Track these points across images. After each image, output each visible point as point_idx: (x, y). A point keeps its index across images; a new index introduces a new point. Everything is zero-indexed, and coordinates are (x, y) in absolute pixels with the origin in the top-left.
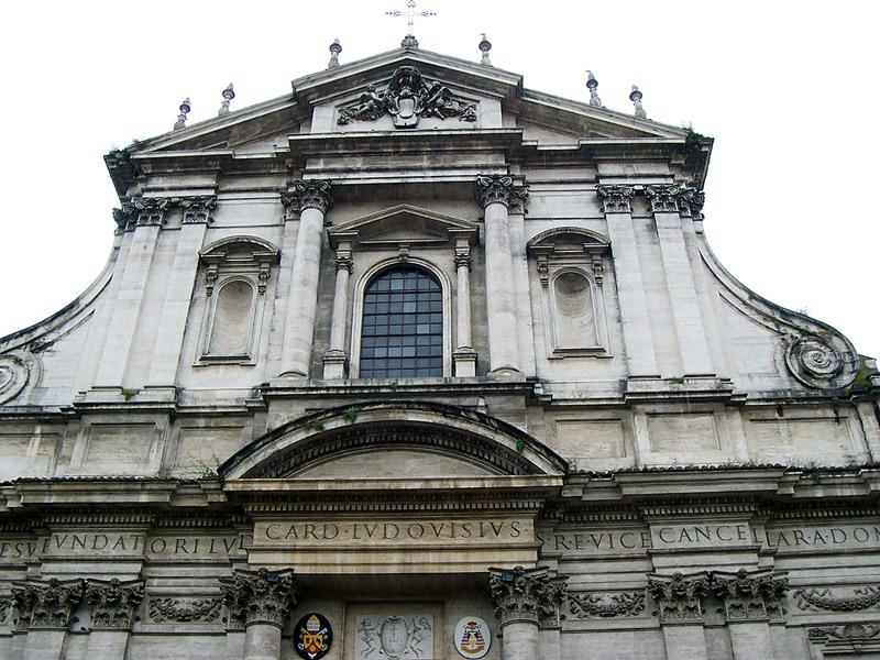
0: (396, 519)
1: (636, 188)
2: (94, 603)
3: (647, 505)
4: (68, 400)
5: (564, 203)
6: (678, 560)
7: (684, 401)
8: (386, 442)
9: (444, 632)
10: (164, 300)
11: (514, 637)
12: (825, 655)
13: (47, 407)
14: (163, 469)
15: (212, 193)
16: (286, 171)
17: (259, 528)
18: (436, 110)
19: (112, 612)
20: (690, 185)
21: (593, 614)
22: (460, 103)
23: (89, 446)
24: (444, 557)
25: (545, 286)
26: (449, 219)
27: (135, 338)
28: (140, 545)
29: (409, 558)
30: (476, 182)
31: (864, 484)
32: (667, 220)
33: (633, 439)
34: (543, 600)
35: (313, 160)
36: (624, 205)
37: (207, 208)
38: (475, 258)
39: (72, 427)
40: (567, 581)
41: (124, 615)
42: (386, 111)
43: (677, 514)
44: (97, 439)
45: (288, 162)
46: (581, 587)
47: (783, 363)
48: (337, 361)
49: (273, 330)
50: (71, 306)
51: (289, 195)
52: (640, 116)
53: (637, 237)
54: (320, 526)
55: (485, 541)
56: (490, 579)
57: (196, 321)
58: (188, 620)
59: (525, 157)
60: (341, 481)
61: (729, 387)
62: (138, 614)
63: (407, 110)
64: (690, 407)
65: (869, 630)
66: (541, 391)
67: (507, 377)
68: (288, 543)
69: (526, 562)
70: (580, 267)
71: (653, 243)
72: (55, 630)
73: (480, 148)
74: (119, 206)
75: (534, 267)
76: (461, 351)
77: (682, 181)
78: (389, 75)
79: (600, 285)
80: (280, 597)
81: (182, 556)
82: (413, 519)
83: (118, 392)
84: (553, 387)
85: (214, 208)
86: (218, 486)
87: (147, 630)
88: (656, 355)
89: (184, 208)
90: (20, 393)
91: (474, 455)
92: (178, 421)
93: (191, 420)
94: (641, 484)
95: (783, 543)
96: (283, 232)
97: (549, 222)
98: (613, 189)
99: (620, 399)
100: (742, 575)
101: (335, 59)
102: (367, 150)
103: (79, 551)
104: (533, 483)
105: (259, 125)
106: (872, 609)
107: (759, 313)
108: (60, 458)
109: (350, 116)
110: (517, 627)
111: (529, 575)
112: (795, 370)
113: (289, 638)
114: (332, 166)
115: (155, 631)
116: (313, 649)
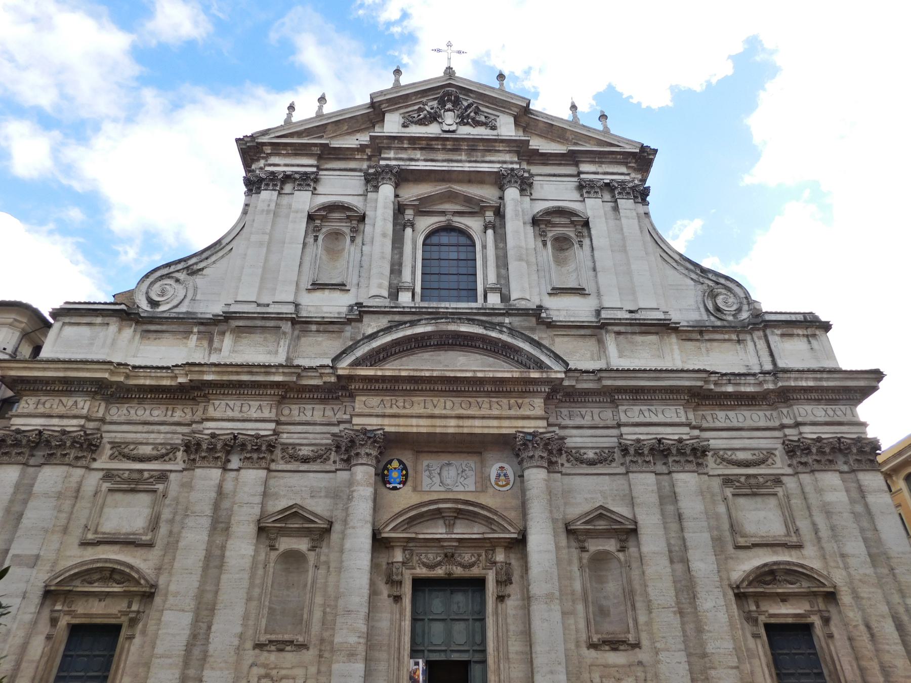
2: (242, 450)
4: (216, 309)
8: (445, 344)
9: (482, 473)
10: (284, 243)
12: (734, 495)
13: (201, 313)
14: (288, 359)
15: (314, 169)
19: (255, 456)
20: (641, 181)
22: (486, 117)
25: (545, 244)
27: (264, 268)
28: (274, 411)
29: (461, 422)
31: (760, 384)
32: (626, 204)
34: (550, 452)
36: (597, 192)
37: (312, 180)
39: (222, 327)
40: (566, 441)
42: (435, 119)
43: (637, 399)
45: (368, 151)
46: (573, 445)
48: (407, 289)
52: (606, 131)
53: (605, 214)
54: (401, 399)
55: (512, 413)
56: (516, 438)
58: (308, 462)
59: (530, 157)
61: (668, 317)
63: (449, 119)
64: (644, 328)
65: (761, 480)
67: (523, 304)
68: (379, 411)
69: (540, 428)
70: (568, 233)
75: (537, 232)
78: (437, 94)
79: (581, 246)
81: (303, 418)
83: (255, 305)
84: (551, 313)
85: (316, 180)
86: (331, 371)
87: (280, 469)
89: (296, 179)
90: (181, 302)
92: (298, 326)
94: (615, 378)
96: (366, 200)
97: (546, 202)
98: (590, 181)
99: (597, 322)
100: (680, 441)
101: (397, 81)
102: (424, 146)
103: (230, 414)
104: (545, 375)
106: (763, 466)
110: (534, 471)
112: (710, 307)
115: (285, 469)
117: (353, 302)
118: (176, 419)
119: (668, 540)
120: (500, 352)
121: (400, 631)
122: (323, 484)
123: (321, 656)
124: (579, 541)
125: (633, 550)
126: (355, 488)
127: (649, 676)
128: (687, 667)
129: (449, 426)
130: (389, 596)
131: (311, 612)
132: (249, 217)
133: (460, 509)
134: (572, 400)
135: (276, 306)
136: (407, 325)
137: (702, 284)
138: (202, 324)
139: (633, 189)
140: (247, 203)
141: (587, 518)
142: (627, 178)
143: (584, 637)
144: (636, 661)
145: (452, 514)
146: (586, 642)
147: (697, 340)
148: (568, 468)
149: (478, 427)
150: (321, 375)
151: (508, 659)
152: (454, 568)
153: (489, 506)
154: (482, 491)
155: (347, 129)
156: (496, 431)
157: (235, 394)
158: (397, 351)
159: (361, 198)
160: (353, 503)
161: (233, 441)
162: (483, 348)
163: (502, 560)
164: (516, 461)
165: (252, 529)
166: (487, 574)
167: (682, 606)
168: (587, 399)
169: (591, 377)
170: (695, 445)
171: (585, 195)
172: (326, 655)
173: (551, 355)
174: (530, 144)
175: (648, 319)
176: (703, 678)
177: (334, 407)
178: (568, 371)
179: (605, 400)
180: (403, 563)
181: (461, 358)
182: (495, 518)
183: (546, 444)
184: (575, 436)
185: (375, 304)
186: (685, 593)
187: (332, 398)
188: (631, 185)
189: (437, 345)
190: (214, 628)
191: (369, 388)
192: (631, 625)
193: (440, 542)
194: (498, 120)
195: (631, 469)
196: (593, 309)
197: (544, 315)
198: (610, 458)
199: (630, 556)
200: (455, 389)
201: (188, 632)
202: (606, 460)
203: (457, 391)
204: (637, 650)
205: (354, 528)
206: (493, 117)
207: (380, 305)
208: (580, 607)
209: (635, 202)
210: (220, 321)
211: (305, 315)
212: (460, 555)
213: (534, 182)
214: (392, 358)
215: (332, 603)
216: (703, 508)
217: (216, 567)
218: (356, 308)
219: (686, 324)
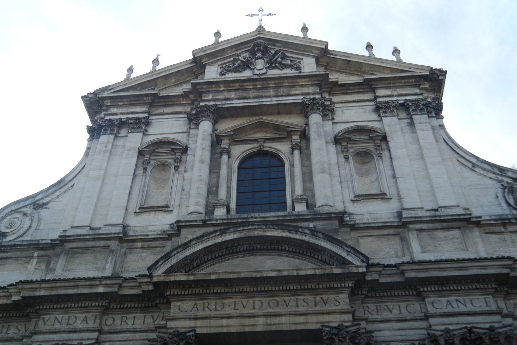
0: (261, 297)
1: (400, 102)
4: (55, 236)
5: (355, 113)
6: (446, 320)
8: (253, 250)
14: (113, 273)
15: (146, 115)
16: (190, 102)
17: (173, 306)
20: (433, 99)
22: (291, 61)
24: (293, 319)
25: (347, 158)
26: (288, 123)
27: (98, 198)
28: (98, 321)
29: (269, 320)
32: (419, 119)
33: (409, 246)
35: (205, 95)
36: (391, 111)
37: (144, 123)
39: (58, 250)
40: (374, 334)
43: (443, 290)
44: (73, 257)
46: (382, 339)
48: (222, 206)
49: (183, 190)
50: (60, 182)
52: (399, 61)
53: (402, 129)
54: (213, 302)
55: (318, 308)
56: (322, 333)
57: (137, 187)
60: (225, 273)
61: (469, 212)
63: (260, 65)
64: (445, 224)
66: (348, 219)
67: (327, 209)
68: (192, 314)
69: (346, 322)
71: (412, 133)
73: (304, 83)
74: (91, 125)
76: (297, 197)
77: (428, 97)
79: (381, 157)
81: (125, 327)
82: (272, 297)
83: (89, 228)
84: (355, 217)
85: (148, 123)
86: (148, 280)
88: (420, 196)
89: (130, 124)
90: (25, 232)
91: (309, 256)
92: (125, 245)
93: (131, 244)
96: (189, 136)
98: (386, 102)
99: (398, 222)
100: (492, 329)
102: (237, 88)
103: (57, 326)
104: (346, 271)
109: (227, 70)
111: (348, 329)
114: (217, 97)
117: (173, 221)
118: (10, 335)
120: (305, 253)
134: (378, 295)
135: (107, 228)
136: (217, 234)
137: (502, 181)
138: (42, 249)
139: (427, 105)
140: (89, 146)
142: (421, 97)
147: (502, 232)
155: (175, 82)
157: (63, 308)
158: (210, 258)
159: (185, 135)
162: (288, 251)
169: (394, 271)
170: (508, 333)
173: (352, 251)
174: (330, 77)
175: (447, 216)
178: (369, 266)
181: (268, 262)
184: (384, 330)
185: (192, 219)
187: (152, 306)
188: (424, 102)
189: (247, 250)
191: (183, 293)
194: (302, 62)
196: (395, 211)
206: (297, 60)
209: (429, 117)
210: (57, 245)
211: (132, 234)
213: (335, 109)
214: (205, 265)
218: (175, 225)
219: (488, 218)
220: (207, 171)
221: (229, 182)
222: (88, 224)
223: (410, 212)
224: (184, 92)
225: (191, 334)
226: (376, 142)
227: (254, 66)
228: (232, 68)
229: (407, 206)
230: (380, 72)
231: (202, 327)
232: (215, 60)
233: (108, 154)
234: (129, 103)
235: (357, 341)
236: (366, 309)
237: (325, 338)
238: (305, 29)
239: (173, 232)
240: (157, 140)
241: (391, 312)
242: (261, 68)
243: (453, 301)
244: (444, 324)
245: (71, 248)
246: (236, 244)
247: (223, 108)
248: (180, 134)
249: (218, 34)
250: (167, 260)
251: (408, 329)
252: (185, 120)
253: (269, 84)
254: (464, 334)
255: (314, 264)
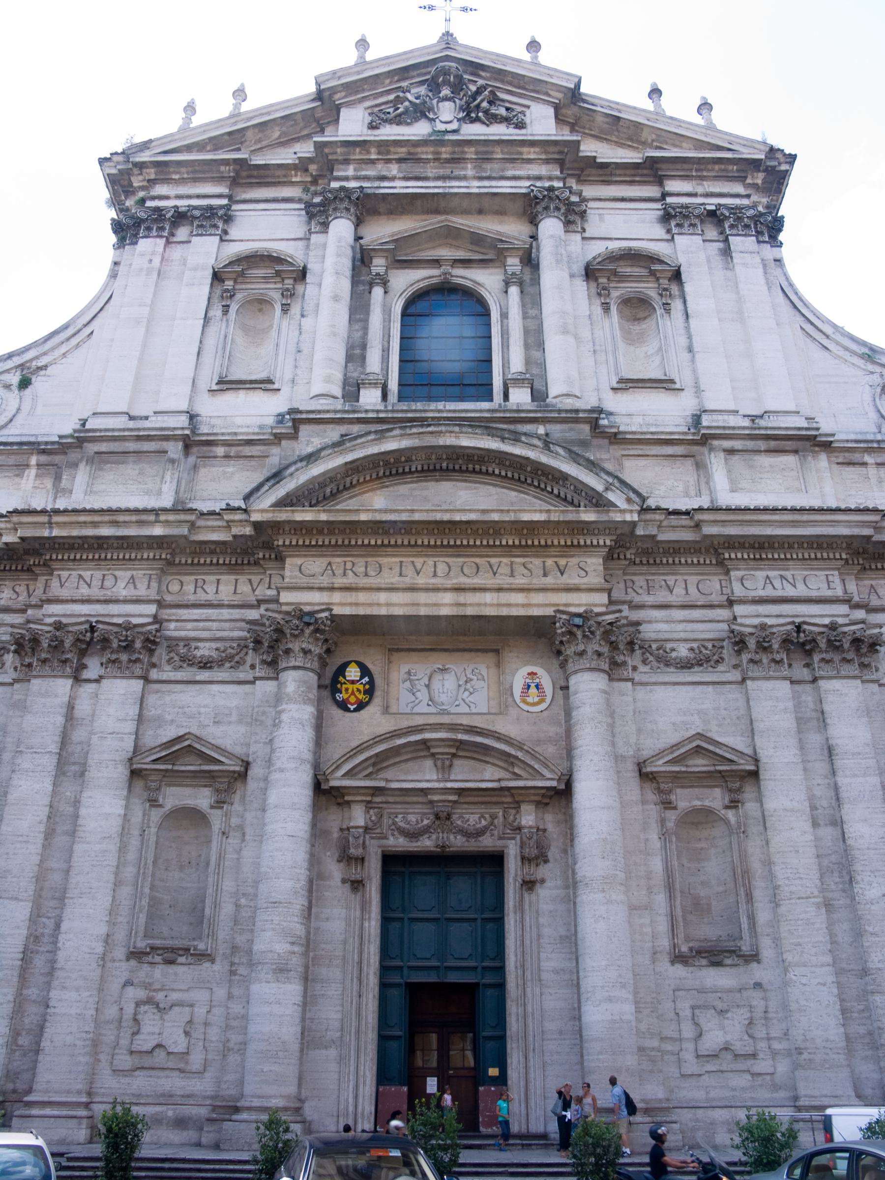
1: (709, 208)
2: (104, 649)
3: (728, 548)
4: (67, 427)
6: (762, 609)
7: (768, 437)
8: (435, 470)
11: (582, 687)
14: (177, 501)
15: (225, 202)
16: (309, 179)
18: (480, 114)
19: (124, 657)
20: (767, 207)
21: (667, 665)
22: (507, 109)
23: (93, 478)
24: (505, 597)
25: (606, 308)
28: (154, 584)
29: (462, 598)
30: (528, 194)
34: (614, 646)
35: (341, 167)
36: (691, 225)
37: (221, 218)
38: (527, 277)
39: (73, 455)
40: (641, 628)
41: (138, 660)
43: (761, 559)
44: (101, 469)
45: (313, 168)
46: (653, 636)
47: (871, 404)
48: (375, 385)
50: (65, 327)
51: (315, 205)
52: (710, 127)
53: (708, 261)
54: (360, 562)
55: (549, 581)
58: (211, 668)
61: (815, 425)
62: (154, 660)
64: (773, 444)
67: (569, 403)
68: (325, 581)
69: (596, 605)
72: (61, 677)
73: (532, 156)
75: (594, 290)
76: (514, 376)
78: (426, 74)
79: (668, 311)
80: (317, 639)
81: (202, 597)
83: (127, 418)
84: (618, 420)
85: (228, 219)
88: (733, 388)
89: (194, 218)
90: (11, 420)
93: (205, 448)
95: (873, 597)
96: (307, 247)
98: (682, 207)
99: (694, 434)
100: (833, 627)
102: (403, 156)
103: (84, 591)
104: (604, 517)
105: (277, 128)
107: (846, 349)
108: (58, 490)
110: (587, 676)
111: (600, 619)
113: (326, 687)
114: (364, 173)
115: (173, 679)
116: (353, 699)
117: (284, 409)
119: (809, 789)
120: (529, 481)
121: (361, 937)
122: (234, 703)
123: (232, 973)
124: (660, 791)
125: (750, 807)
126: (284, 706)
127: (773, 1005)
128: (835, 991)
129: (442, 605)
130: (344, 881)
131: (216, 905)
132: (120, 281)
133: (461, 742)
134: (651, 561)
135: (160, 418)
138: (44, 452)
139: (757, 219)
140: (117, 260)
141: (675, 755)
142: (745, 202)
143: (664, 943)
144: (752, 982)
145: (447, 750)
146: (670, 953)
148: (643, 673)
149: (491, 605)
150: (229, 526)
151: (540, 980)
152: (452, 837)
153: (512, 736)
154: (501, 713)
155: (280, 137)
156: (521, 612)
158: (354, 482)
159: (301, 244)
160: (281, 731)
161: (88, 634)
162: (500, 475)
163: (530, 823)
164: (555, 663)
165: (121, 773)
166: (507, 847)
167: (830, 895)
168: (677, 560)
169: (684, 521)
170: (858, 635)
171: (675, 230)
172: (242, 970)
174: (582, 148)
175: (779, 428)
176: (862, 1007)
177: (253, 578)
179: (708, 562)
180: (366, 829)
181: (462, 493)
182: (520, 754)
183: (606, 634)
184: (657, 622)
185: (319, 408)
186: (836, 874)
187: (249, 563)
188: (751, 212)
189: (423, 471)
190: (64, 926)
192: (745, 926)
193: (426, 795)
194: (528, 112)
195: (750, 674)
196: (689, 413)
197: (604, 422)
198: (715, 657)
199: (746, 816)
200: (452, 543)
201: (25, 932)
202: (708, 660)
203: (455, 546)
204: (754, 965)
205: (282, 770)
206: (519, 109)
207: (326, 408)
208: (660, 899)
209: (759, 242)
210: (70, 446)
211: (206, 431)
212: (461, 817)
213: (588, 211)
214: (346, 494)
215: (251, 891)
216: (869, 736)
217: (66, 833)
218: (288, 417)
220: (347, 317)
221: (386, 339)
222: (125, 410)
223: (715, 417)
224: (299, 158)
225: (323, 615)
226: (661, 281)
227: (435, 114)
228: (392, 115)
229: (710, 406)
230: (675, 146)
231: (342, 604)
232: (359, 96)
233: (155, 275)
234: (191, 176)
235: (613, 639)
236: (629, 584)
237: (559, 631)
238: (534, 46)
239: (283, 431)
240: (247, 253)
241: (671, 592)
242: (449, 119)
243: (775, 578)
244: (757, 616)
245: (96, 453)
246: (403, 459)
247: (375, 194)
248: (292, 243)
249: (363, 44)
250: (278, 482)
251: (698, 622)
252: (299, 215)
253: (463, 152)
254: (788, 633)
255: (545, 501)
